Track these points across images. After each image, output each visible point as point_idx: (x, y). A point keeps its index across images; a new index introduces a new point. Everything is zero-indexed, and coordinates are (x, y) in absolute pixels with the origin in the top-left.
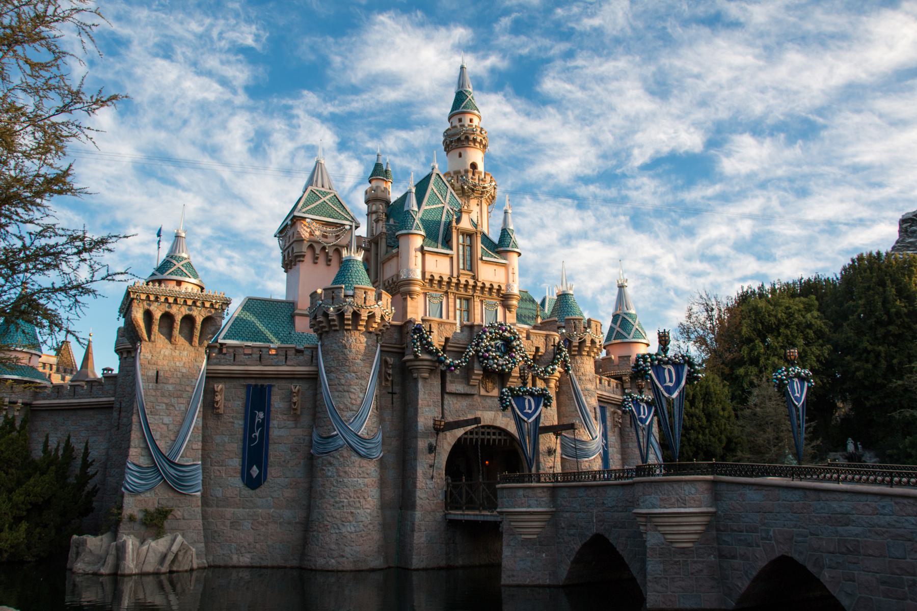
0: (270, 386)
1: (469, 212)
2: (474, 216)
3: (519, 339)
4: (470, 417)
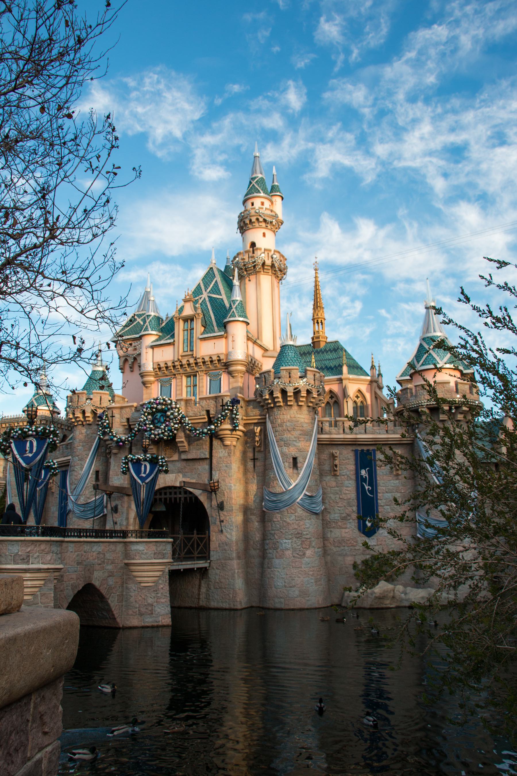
3: (172, 408)
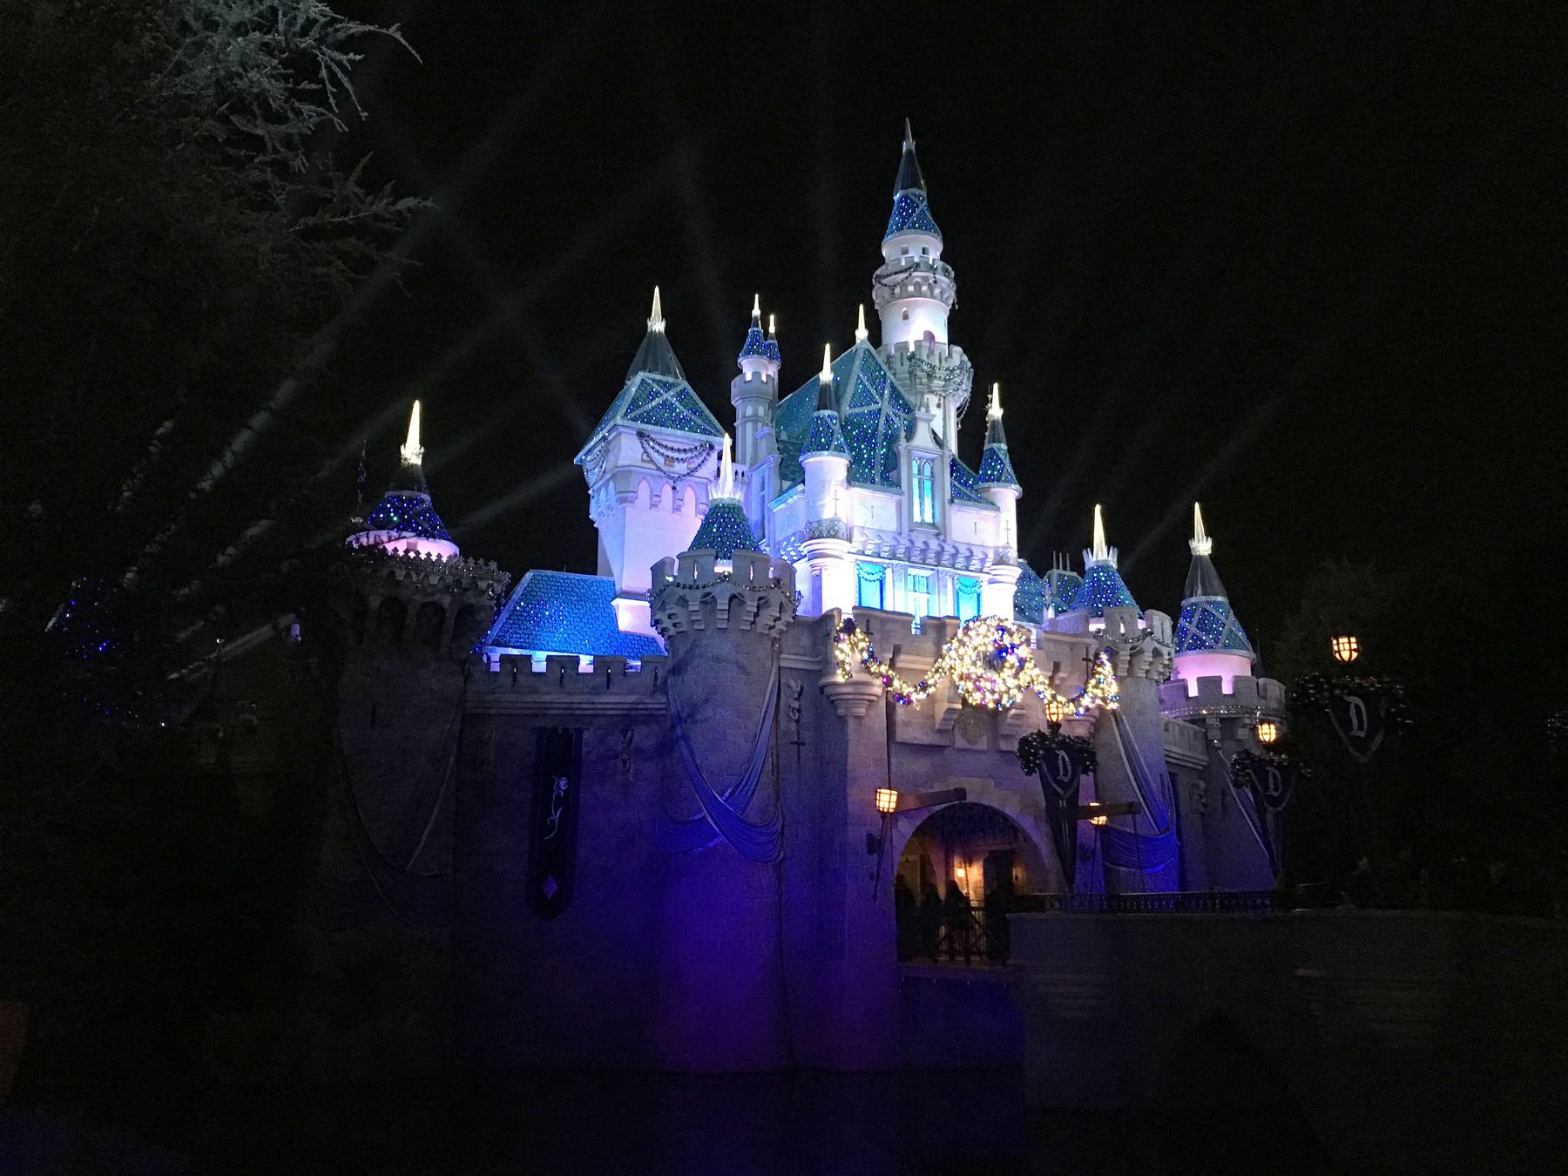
0: (580, 732)
1: (929, 421)
2: (937, 425)
4: (938, 788)
